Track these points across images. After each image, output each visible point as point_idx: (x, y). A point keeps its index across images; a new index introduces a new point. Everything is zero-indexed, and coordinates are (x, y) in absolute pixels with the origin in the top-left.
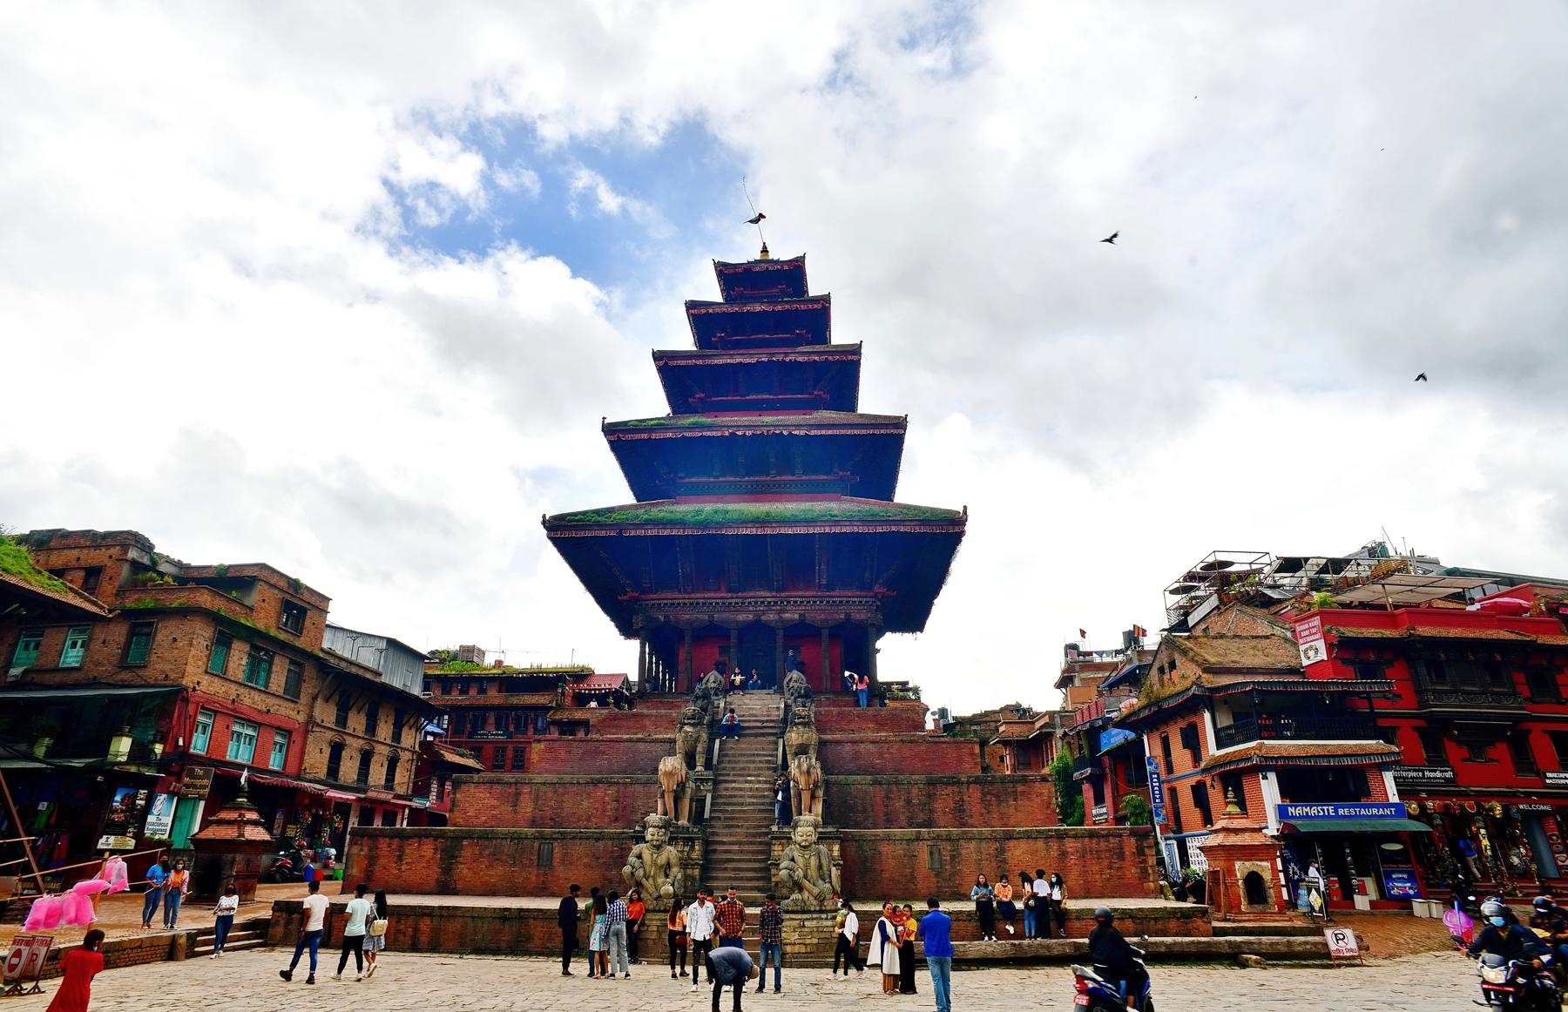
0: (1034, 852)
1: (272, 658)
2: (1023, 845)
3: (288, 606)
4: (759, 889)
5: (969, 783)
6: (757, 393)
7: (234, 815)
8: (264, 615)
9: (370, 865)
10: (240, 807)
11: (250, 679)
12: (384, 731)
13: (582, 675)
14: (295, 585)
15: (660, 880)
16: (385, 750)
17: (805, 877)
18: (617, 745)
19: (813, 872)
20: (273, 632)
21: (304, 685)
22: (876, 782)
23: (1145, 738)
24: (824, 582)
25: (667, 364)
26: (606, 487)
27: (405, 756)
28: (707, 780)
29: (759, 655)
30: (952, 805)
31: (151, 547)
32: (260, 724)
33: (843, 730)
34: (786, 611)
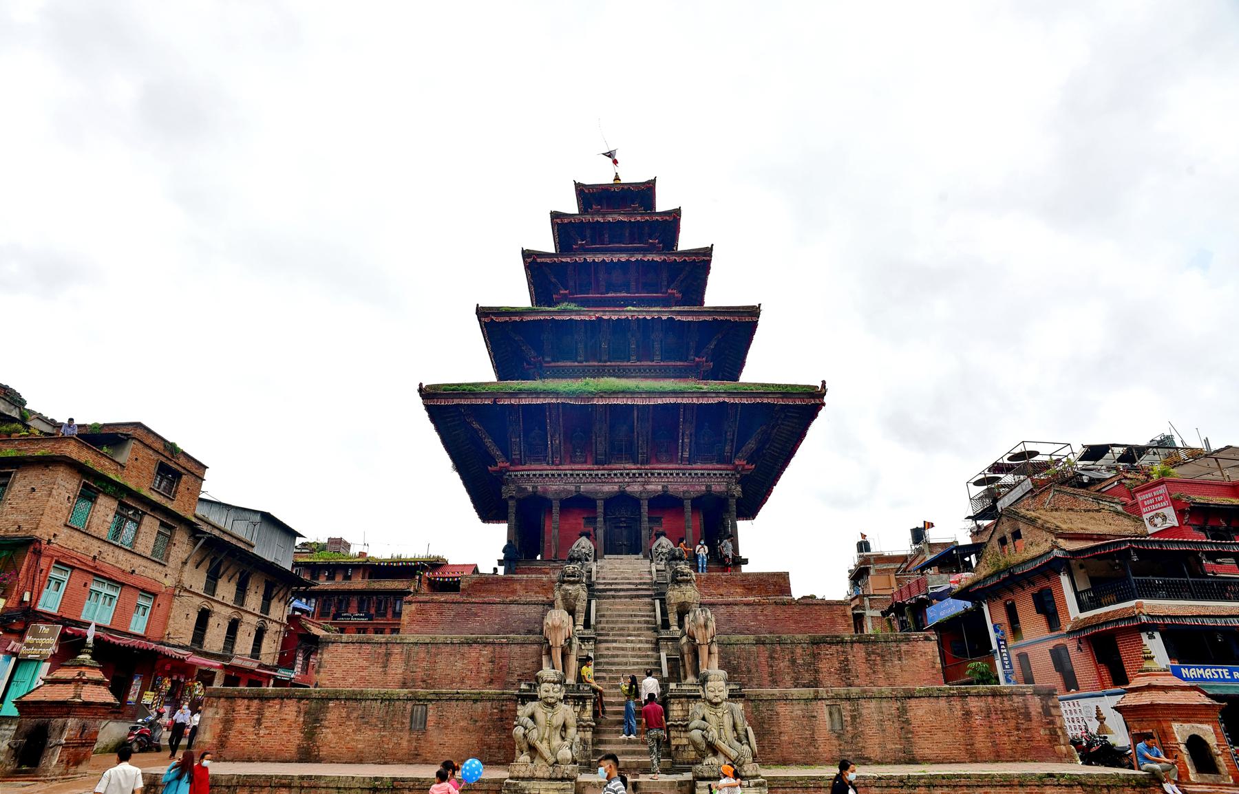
0: (937, 713)
1: (141, 519)
2: (925, 704)
3: (163, 470)
5: (852, 642)
6: (615, 292)
8: (134, 471)
9: (225, 730)
11: (115, 537)
12: (254, 601)
13: (436, 564)
14: (172, 449)
16: (254, 621)
18: (489, 607)
20: (145, 492)
21: (174, 549)
22: (759, 642)
23: (985, 608)
24: (686, 455)
25: (532, 260)
27: (272, 628)
28: (589, 639)
29: (623, 525)
30: (837, 665)
31: (23, 403)
32: (123, 584)
34: (648, 483)
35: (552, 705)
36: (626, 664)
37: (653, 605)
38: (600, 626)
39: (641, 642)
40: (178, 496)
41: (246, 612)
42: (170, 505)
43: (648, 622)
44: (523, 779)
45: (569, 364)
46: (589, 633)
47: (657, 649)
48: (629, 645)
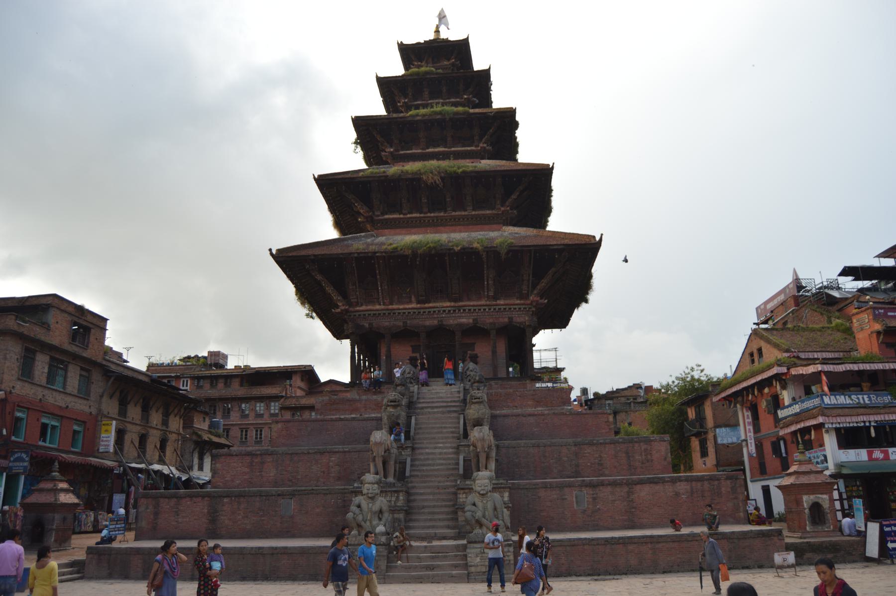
1: (66, 366)
4: (448, 527)
6: (435, 147)
7: (49, 485)
8: (58, 333)
10: (54, 480)
12: (156, 418)
15: (375, 522)
17: (484, 516)
19: (490, 512)
24: (491, 294)
26: (319, 226)
27: (173, 437)
32: (62, 417)
33: (508, 407)
35: (372, 498)
36: (434, 465)
37: (459, 418)
38: (417, 436)
39: (446, 448)
40: (90, 346)
41: (151, 427)
42: (84, 355)
43: (452, 432)
44: (354, 545)
46: (409, 443)
47: (457, 453)
48: (437, 451)
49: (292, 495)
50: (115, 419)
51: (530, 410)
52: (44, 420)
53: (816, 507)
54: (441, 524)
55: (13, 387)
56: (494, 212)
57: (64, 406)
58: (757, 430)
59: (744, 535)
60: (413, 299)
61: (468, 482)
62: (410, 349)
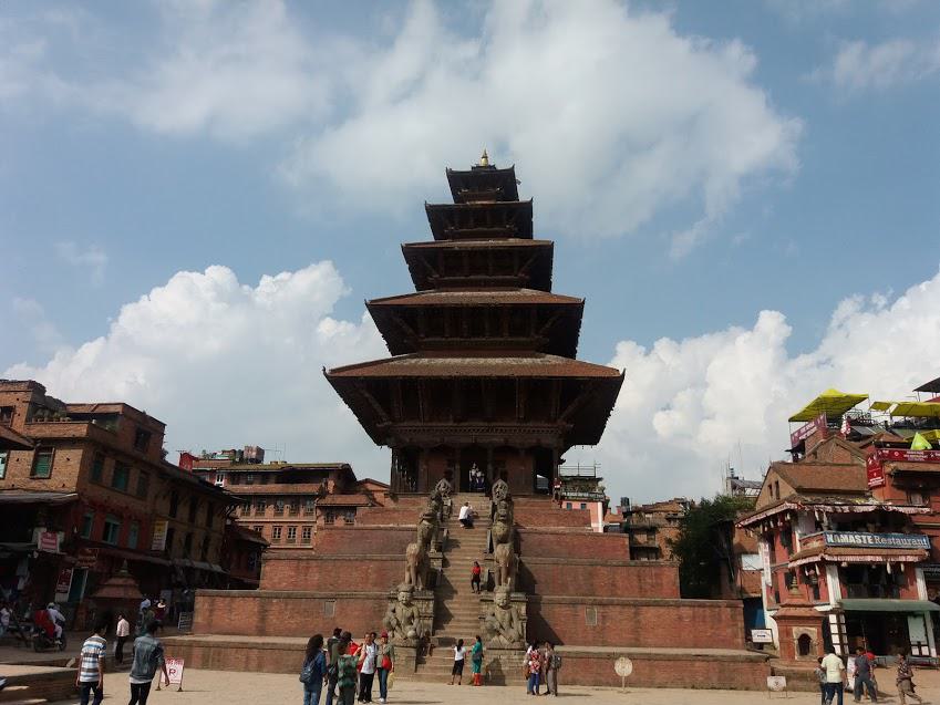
2: (652, 610)
3: (138, 432)
10: (122, 577)
12: (201, 517)
42: (144, 458)
43: (480, 546)
45: (438, 339)
48: (465, 563)
49: (333, 598)
50: (164, 519)
51: (553, 528)
52: (108, 520)
53: (804, 641)
54: (465, 631)
55: (85, 490)
56: (529, 340)
57: (124, 505)
58: (773, 560)
59: (734, 659)
60: (451, 417)
61: (490, 594)
62: (446, 462)
